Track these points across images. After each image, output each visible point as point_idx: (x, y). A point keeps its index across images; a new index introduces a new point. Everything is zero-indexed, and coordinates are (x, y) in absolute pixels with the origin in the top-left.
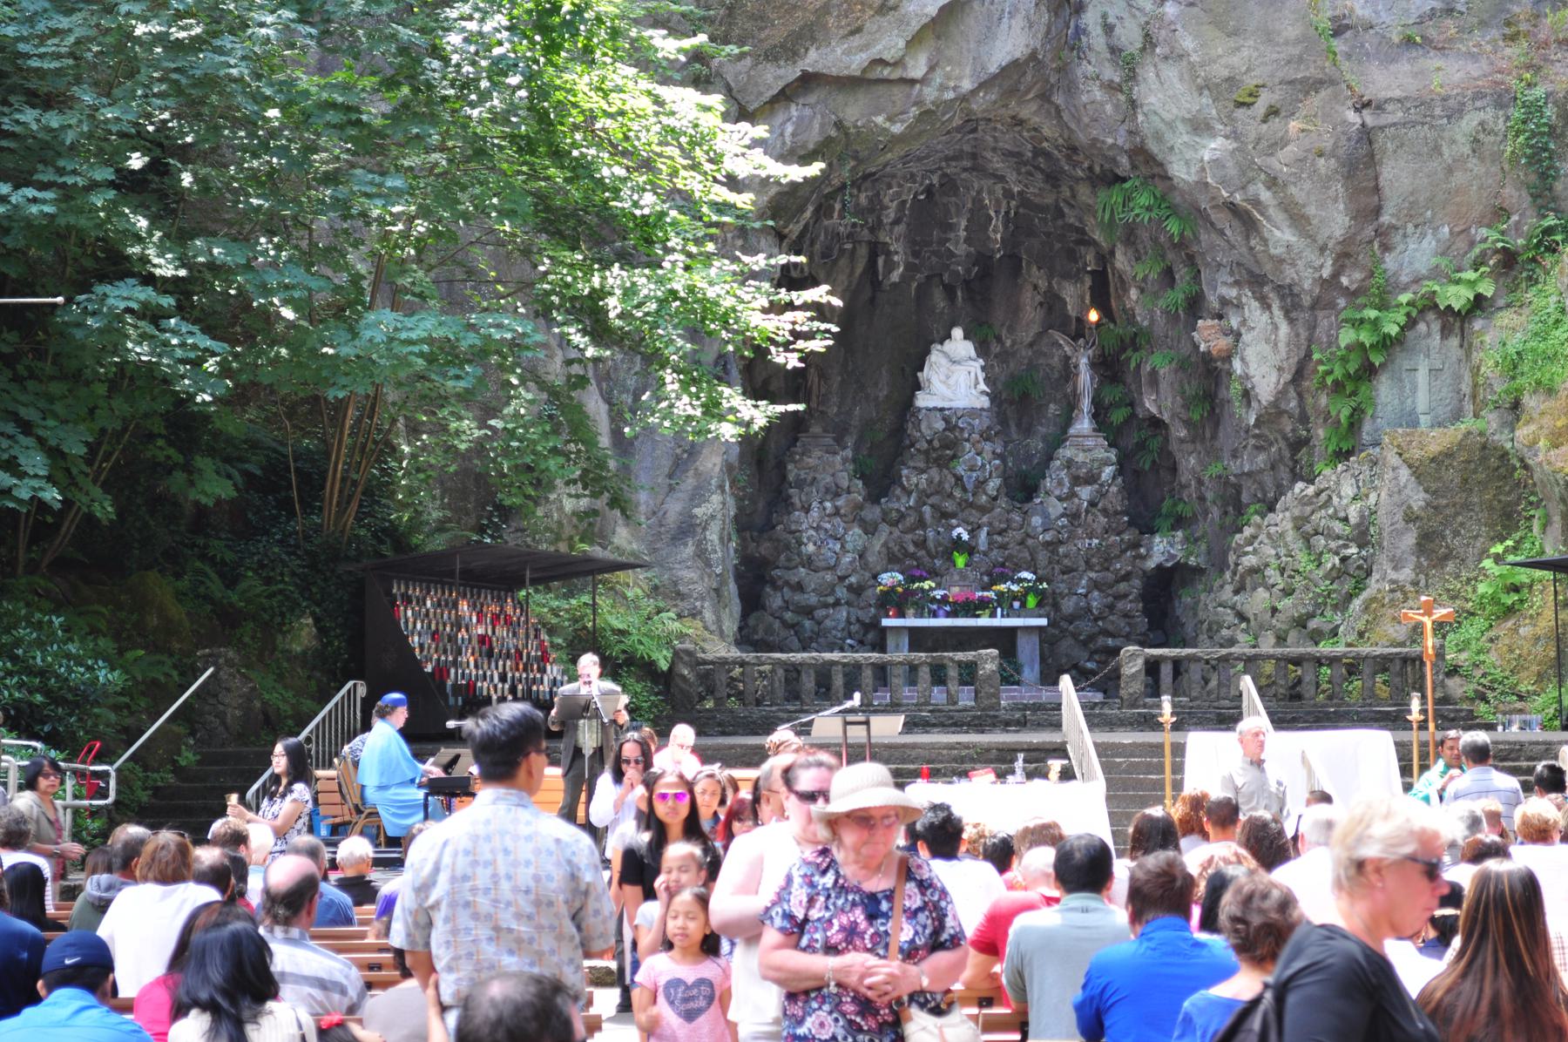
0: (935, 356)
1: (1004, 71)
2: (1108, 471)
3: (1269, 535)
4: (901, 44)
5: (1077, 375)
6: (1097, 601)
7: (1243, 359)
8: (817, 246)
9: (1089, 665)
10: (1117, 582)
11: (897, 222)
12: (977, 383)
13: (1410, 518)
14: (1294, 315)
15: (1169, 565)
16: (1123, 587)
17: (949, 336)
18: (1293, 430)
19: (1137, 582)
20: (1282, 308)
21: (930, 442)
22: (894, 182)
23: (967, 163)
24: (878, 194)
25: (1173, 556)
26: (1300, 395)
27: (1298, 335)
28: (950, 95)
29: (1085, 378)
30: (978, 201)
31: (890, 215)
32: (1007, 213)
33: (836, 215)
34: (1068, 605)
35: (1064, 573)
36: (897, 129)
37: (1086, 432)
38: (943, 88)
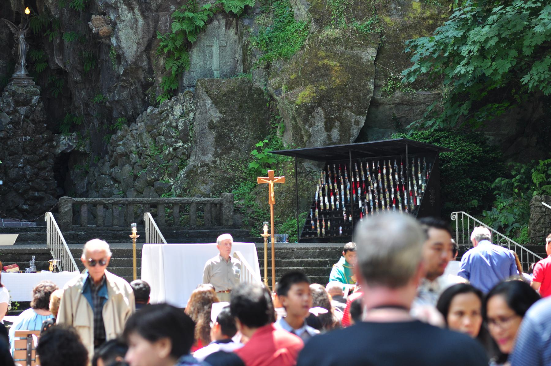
2: (36, 98)
3: (132, 136)
5: (18, 44)
7: (117, 38)
9: (25, 207)
10: (40, 160)
13: (212, 126)
14: (146, 14)
15: (69, 151)
18: (145, 78)
19: (51, 161)
20: (140, 10)
25: (70, 147)
26: (149, 59)
29: (22, 46)
34: (13, 173)
35: (10, 155)
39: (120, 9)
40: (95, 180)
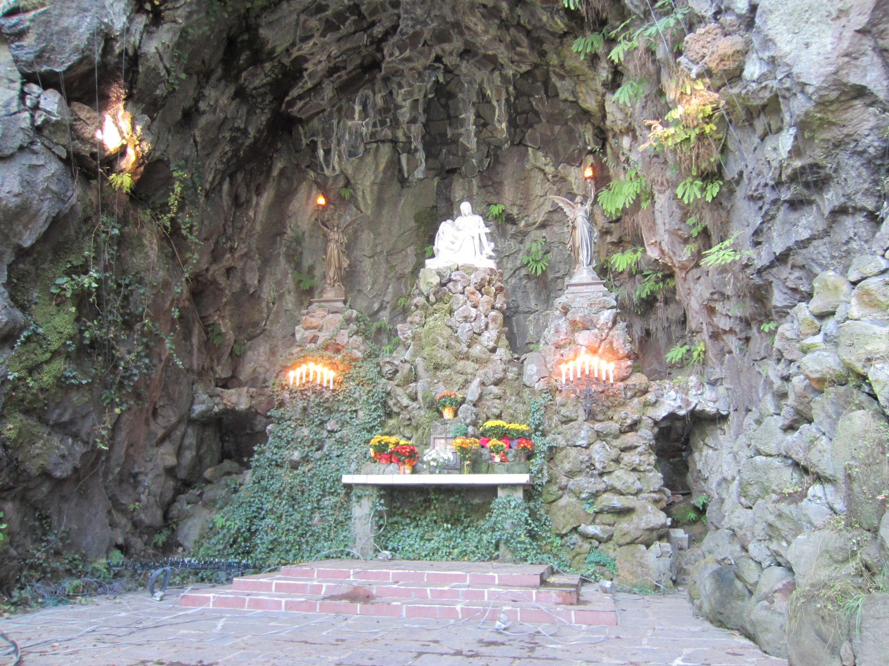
0: (445, 227)
2: (606, 316)
6: (600, 453)
8: (343, 145)
10: (623, 432)
11: (413, 121)
16: (630, 438)
17: (459, 213)
21: (427, 298)
22: (403, 82)
23: (457, 44)
24: (391, 93)
31: (405, 114)
33: (357, 116)
37: (585, 281)
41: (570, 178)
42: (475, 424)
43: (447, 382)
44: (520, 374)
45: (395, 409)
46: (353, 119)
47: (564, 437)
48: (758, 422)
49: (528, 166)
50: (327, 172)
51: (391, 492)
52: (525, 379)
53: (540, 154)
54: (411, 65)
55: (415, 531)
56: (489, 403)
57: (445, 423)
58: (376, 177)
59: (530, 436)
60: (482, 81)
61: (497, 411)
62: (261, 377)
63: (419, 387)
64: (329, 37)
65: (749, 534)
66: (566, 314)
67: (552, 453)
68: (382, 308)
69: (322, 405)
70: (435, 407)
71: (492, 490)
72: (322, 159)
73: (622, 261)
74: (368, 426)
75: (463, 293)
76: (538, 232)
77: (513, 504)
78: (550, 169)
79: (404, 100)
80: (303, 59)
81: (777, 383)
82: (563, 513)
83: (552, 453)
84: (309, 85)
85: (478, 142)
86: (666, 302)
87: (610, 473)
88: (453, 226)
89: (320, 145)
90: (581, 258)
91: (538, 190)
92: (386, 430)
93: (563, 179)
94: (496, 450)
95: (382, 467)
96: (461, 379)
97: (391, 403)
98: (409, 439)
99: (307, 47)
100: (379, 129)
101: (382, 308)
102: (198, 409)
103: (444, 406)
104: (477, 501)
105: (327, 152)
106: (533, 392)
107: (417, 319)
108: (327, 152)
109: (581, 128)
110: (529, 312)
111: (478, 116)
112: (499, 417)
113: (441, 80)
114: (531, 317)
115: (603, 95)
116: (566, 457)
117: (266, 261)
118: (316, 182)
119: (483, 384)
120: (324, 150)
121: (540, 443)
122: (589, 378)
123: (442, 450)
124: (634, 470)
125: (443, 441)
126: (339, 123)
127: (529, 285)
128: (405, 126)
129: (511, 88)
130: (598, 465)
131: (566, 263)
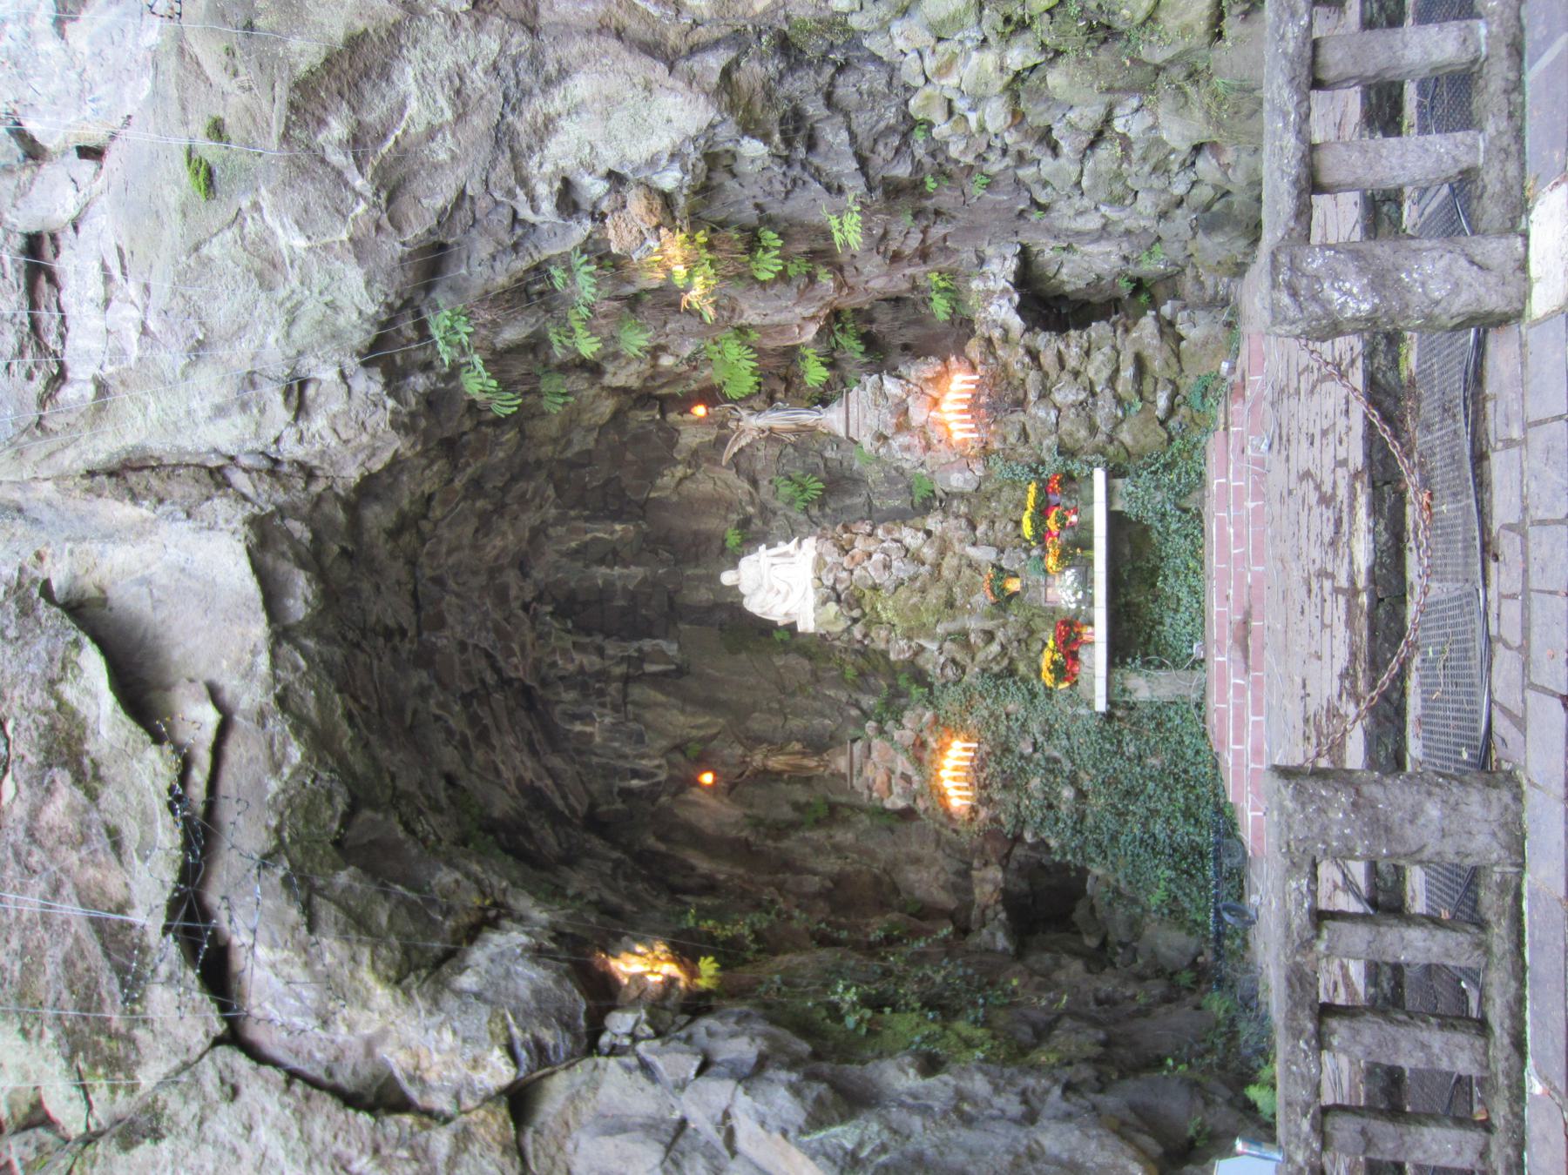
1: (258, 570)
2: (891, 386)
3: (945, 68)
4: (152, 753)
6: (1066, 394)
7: (652, 162)
8: (627, 750)
10: (1040, 367)
11: (600, 651)
12: (785, 554)
16: (1048, 359)
17: (735, 587)
21: (855, 621)
22: (548, 660)
23: (511, 577)
24: (562, 678)
26: (694, 50)
27: (585, 57)
28: (264, 661)
29: (777, 419)
30: (574, 554)
31: (591, 661)
32: (587, 519)
33: (588, 729)
36: (296, 753)
37: (843, 416)
38: (249, 674)
39: (562, 164)
40: (1096, 208)
41: (694, 445)
42: (1027, 550)
43: (970, 591)
44: (962, 496)
45: (1005, 662)
46: (592, 734)
47: (1045, 436)
48: (1045, 184)
49: (675, 498)
50: (663, 776)
51: (1119, 653)
52: (969, 489)
53: (659, 482)
54: (529, 647)
55: (1168, 621)
56: (1000, 535)
57: (1025, 588)
58: (674, 706)
59: (1043, 481)
60: (558, 552)
61: (1010, 526)
62: (952, 878)
63: (973, 624)
64: (495, 741)
65: (1164, 197)
66: (886, 438)
67: (1065, 451)
68: (857, 705)
69: (999, 768)
70: (1004, 601)
71: (1116, 520)
72: (643, 783)
73: (815, 374)
74: (1027, 697)
75: (851, 572)
76: (763, 491)
77: (1131, 489)
78: (680, 471)
79: (573, 660)
80: (520, 781)
81: (1008, 161)
82: (1141, 437)
83: (1065, 451)
84: (549, 782)
85: (637, 564)
86: (871, 321)
87: (1091, 383)
88: (753, 594)
89: (625, 784)
90: (810, 423)
91: (709, 486)
92: (1033, 675)
93: (695, 453)
94: (1062, 519)
95: (1084, 669)
96: (967, 572)
97: (996, 669)
98: (1045, 644)
99: (507, 773)
100: (608, 699)
101: (857, 705)
102: (1001, 942)
103: (1003, 589)
104: (1127, 550)
105: (636, 774)
106: (987, 478)
107: (883, 633)
108: (636, 774)
109: (632, 425)
110: (870, 504)
111: (602, 561)
112: (1018, 524)
113: (549, 608)
114: (877, 503)
115: (603, 388)
116: (1071, 435)
117: (787, 864)
118: (674, 795)
119: (974, 544)
120: (633, 778)
121: (1053, 464)
122: (974, 406)
123: (1063, 592)
124: (1088, 353)
125: (1050, 591)
126: (596, 755)
127: (832, 505)
128: (608, 663)
129: (572, 513)
130: (1082, 396)
131: (806, 455)
